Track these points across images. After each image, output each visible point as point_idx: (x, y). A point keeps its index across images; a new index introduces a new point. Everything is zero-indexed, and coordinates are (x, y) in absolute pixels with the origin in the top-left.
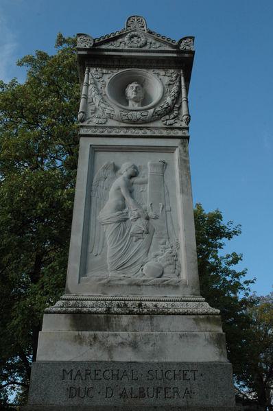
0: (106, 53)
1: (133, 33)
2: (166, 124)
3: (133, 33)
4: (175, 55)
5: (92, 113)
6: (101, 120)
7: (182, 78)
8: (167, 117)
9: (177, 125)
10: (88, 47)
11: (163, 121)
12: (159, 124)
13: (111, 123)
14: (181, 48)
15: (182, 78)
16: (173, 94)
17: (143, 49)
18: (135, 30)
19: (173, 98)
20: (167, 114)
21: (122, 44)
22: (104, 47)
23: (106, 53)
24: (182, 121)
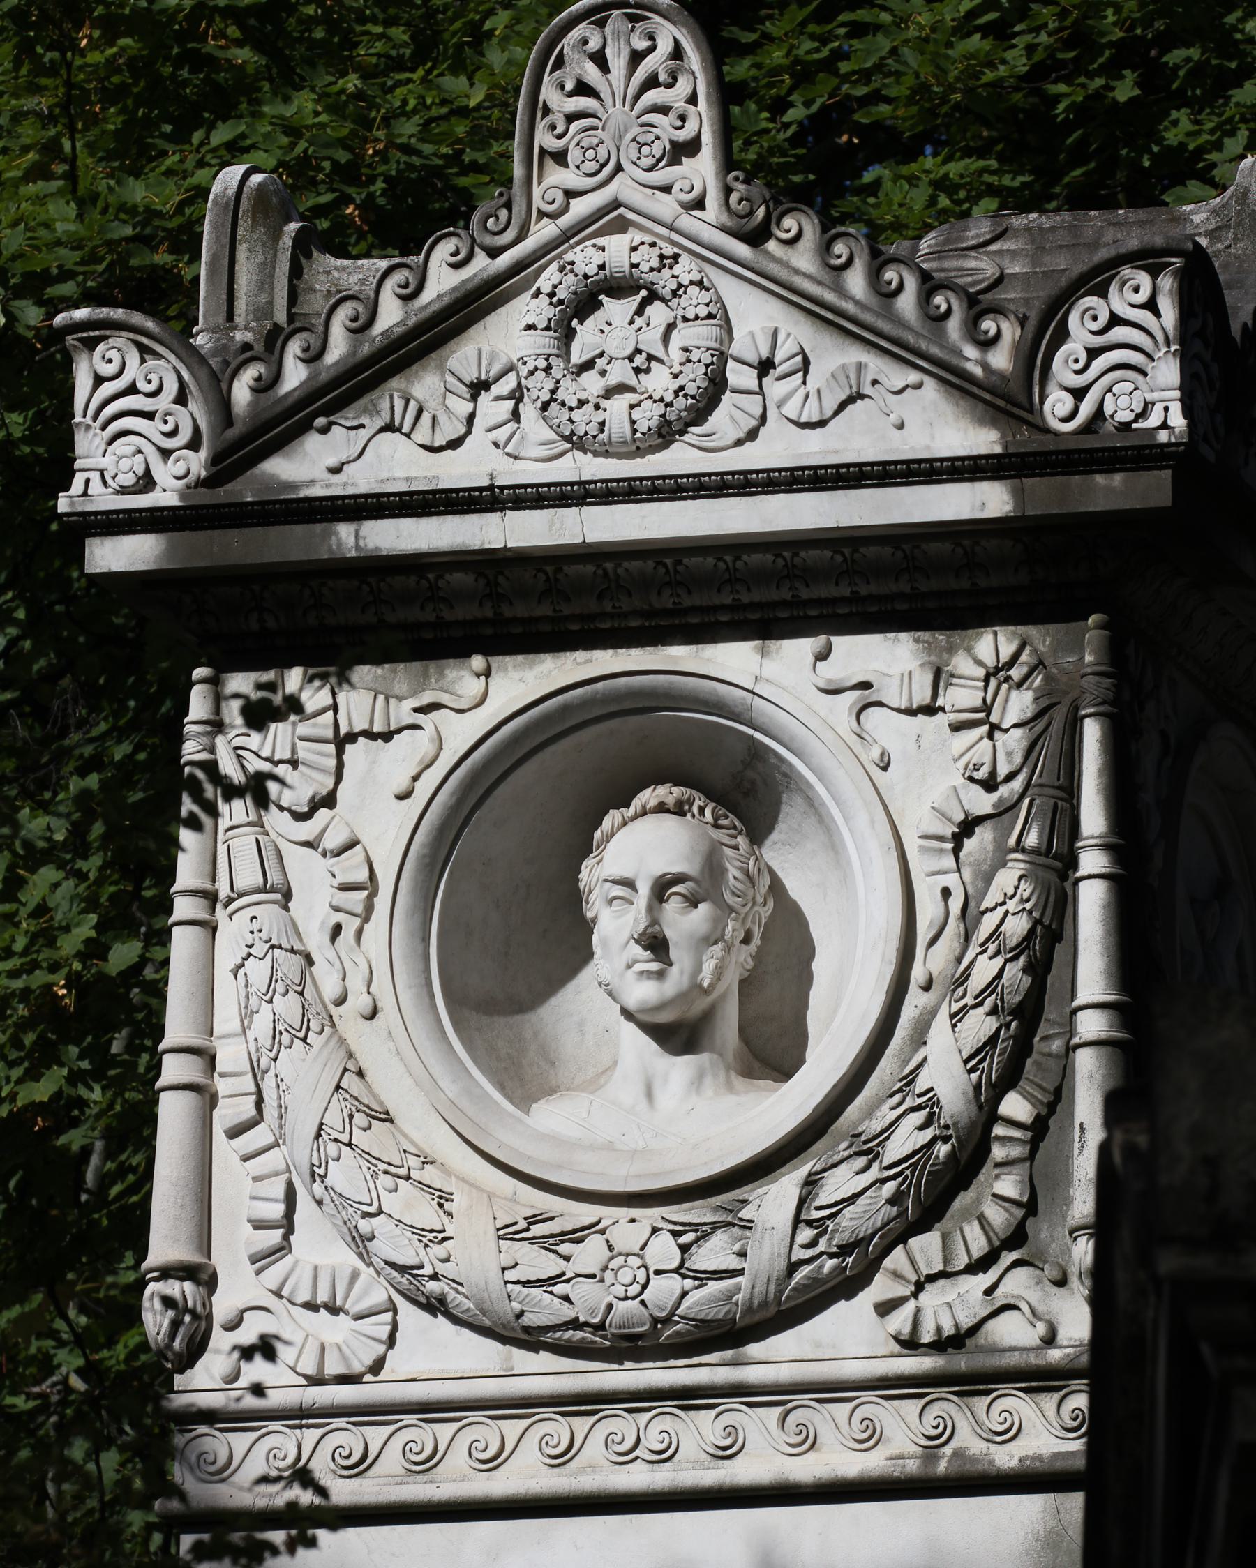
0: (348, 538)
1: (585, 258)
2: (910, 1344)
3: (585, 258)
4: (989, 500)
5: (263, 1259)
6: (350, 1342)
7: (1092, 732)
8: (926, 1247)
9: (1014, 1333)
10: (166, 496)
11: (885, 1308)
12: (847, 1336)
13: (438, 1356)
14: (1056, 404)
15: (1092, 732)
16: (985, 970)
17: (680, 459)
18: (612, 218)
19: (979, 1025)
20: (921, 1225)
21: (492, 409)
22: (308, 466)
23: (348, 538)
24: (1061, 1282)
